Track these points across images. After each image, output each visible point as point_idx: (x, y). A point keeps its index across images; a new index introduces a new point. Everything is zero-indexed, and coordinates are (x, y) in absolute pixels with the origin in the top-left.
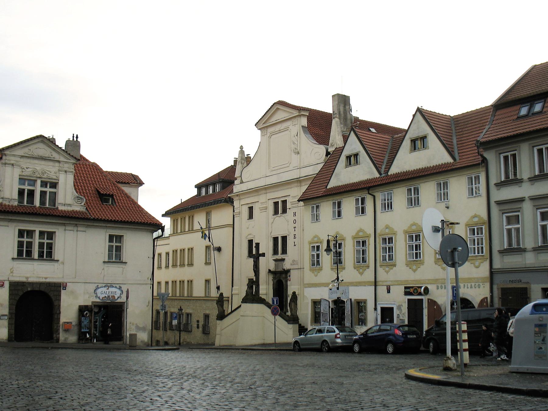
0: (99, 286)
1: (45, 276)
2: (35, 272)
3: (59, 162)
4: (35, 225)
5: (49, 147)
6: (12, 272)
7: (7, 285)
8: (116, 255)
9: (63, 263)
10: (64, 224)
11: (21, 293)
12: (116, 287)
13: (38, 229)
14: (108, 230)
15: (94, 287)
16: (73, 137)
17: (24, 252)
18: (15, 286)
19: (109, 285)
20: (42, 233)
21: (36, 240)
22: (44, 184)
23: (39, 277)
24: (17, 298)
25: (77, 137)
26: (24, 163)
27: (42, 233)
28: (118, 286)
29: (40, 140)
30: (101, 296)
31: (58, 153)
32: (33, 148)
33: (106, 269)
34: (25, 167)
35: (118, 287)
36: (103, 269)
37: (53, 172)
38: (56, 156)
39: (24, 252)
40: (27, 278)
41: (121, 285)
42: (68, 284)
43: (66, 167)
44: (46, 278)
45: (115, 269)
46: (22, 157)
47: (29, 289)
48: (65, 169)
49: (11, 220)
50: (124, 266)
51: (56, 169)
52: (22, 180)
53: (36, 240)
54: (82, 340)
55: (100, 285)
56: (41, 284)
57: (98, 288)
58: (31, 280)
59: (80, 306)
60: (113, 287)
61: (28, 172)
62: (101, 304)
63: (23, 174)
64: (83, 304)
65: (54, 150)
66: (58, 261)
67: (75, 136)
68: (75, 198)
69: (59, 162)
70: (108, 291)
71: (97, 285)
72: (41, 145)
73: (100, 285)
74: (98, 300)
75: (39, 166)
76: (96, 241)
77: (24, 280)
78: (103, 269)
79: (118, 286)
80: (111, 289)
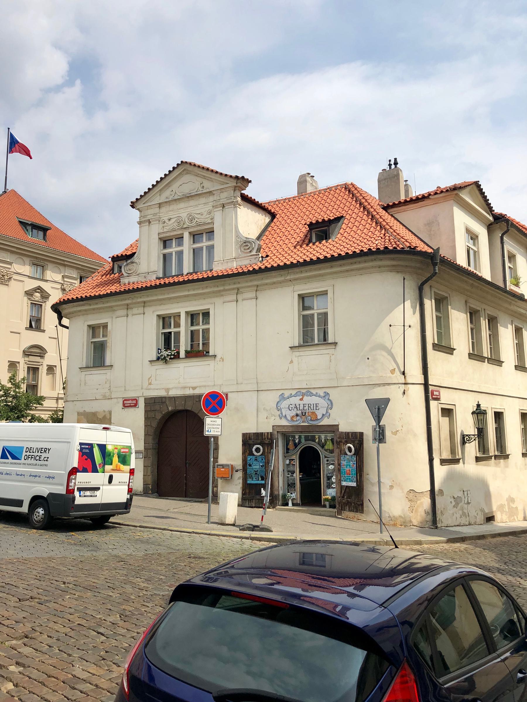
0: (286, 396)
1: (194, 385)
2: (184, 379)
3: (210, 193)
4: (175, 305)
5: (197, 175)
6: (150, 384)
7: (142, 403)
8: (314, 332)
9: (222, 359)
10: (218, 294)
11: (159, 416)
12: (316, 395)
13: (182, 309)
14: (297, 287)
15: (274, 397)
16: (390, 165)
17: (168, 350)
18: (152, 404)
19: (304, 391)
20: (193, 317)
21: (184, 330)
22: (195, 236)
24: (154, 424)
25: (396, 163)
26: (166, 213)
27: (193, 317)
28: (321, 392)
30: (290, 414)
31: (210, 179)
32: (175, 186)
33: (295, 360)
34: (166, 219)
35: (322, 394)
36: (292, 362)
37: (206, 213)
38: (209, 186)
39: (168, 350)
40: (167, 390)
41: (327, 390)
42: (230, 395)
44: (194, 388)
45: (315, 358)
46: (160, 205)
47: (170, 409)
48: (222, 202)
50: (331, 351)
51: (209, 207)
52: (165, 242)
53: (184, 330)
54: (250, 500)
55: (287, 394)
56: (186, 398)
57: (282, 398)
58: (173, 393)
59: (244, 435)
60: (311, 395)
62: (291, 430)
63: (165, 230)
64: (252, 429)
65: (204, 177)
67: (392, 162)
68: (241, 246)
69: (210, 193)
70: (302, 403)
71: (280, 392)
72: (186, 178)
73: (287, 394)
74: (284, 423)
75: (183, 212)
77: (162, 393)
78: (292, 362)
79: (321, 392)
80: (307, 400)
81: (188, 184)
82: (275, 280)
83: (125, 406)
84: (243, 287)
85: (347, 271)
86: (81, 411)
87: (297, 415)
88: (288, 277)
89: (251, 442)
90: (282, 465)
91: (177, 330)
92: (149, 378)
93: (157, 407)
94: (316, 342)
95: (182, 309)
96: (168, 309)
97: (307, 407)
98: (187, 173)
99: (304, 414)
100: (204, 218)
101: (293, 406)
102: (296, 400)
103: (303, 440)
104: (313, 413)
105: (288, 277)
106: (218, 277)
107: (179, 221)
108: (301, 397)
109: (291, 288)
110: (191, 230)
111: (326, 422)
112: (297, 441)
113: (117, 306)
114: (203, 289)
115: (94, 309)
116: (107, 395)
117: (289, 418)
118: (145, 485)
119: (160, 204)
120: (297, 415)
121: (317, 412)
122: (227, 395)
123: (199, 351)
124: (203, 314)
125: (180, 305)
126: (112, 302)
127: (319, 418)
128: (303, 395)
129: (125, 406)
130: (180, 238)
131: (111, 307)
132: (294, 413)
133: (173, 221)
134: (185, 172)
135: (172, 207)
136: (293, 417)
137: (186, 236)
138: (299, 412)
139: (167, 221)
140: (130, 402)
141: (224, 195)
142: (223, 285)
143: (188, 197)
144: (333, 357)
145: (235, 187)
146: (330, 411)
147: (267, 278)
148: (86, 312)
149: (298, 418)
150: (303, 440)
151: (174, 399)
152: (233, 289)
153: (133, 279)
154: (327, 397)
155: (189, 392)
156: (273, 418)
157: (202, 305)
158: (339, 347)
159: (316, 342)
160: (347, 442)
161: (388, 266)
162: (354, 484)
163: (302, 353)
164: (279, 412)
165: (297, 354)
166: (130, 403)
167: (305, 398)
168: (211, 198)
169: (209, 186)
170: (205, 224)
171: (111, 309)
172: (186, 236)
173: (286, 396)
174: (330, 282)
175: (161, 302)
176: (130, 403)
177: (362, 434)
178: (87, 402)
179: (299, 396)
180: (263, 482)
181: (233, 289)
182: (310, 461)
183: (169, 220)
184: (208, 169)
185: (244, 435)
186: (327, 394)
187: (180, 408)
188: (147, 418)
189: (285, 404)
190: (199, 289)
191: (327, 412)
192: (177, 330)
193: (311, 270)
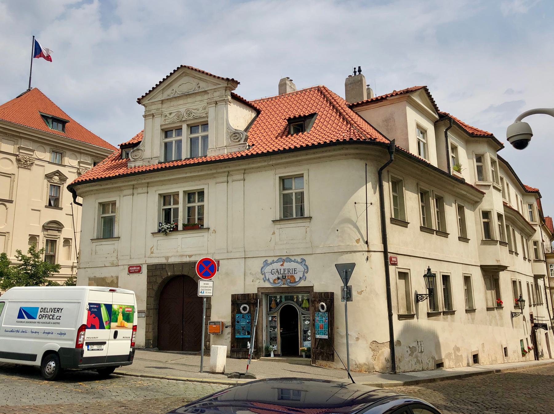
0: (269, 262)
2: (182, 248)
5: (194, 77)
6: (152, 253)
7: (145, 270)
8: (292, 209)
9: (215, 231)
10: (212, 176)
11: (159, 281)
12: (295, 261)
13: (180, 189)
14: (278, 171)
16: (355, 72)
17: (168, 224)
18: (154, 270)
19: (284, 258)
20: (190, 195)
21: (181, 206)
22: (192, 128)
23: (182, 256)
24: (156, 288)
25: (360, 71)
26: (167, 109)
28: (299, 259)
29: (180, 72)
30: (272, 277)
32: (175, 86)
33: (277, 232)
34: (167, 113)
35: (299, 261)
36: (274, 233)
38: (204, 86)
39: (168, 224)
40: (167, 258)
42: (221, 262)
43: (216, 95)
44: (190, 256)
45: (293, 230)
46: (162, 102)
47: (169, 274)
49: (148, 185)
50: (307, 224)
51: (204, 104)
52: (167, 133)
53: (181, 206)
54: (238, 352)
55: (270, 260)
57: (266, 264)
58: (172, 260)
59: (233, 296)
60: (291, 261)
61: (170, 121)
63: (167, 123)
64: (240, 291)
65: (200, 79)
66: (208, 229)
67: (357, 70)
68: (231, 137)
70: (282, 268)
71: (265, 259)
72: (185, 79)
73: (270, 260)
75: (181, 107)
76: (261, 191)
77: (163, 261)
78: (274, 233)
79: (299, 259)
80: (287, 265)
81: (186, 84)
82: (259, 165)
83: (130, 272)
84: (233, 171)
85: (320, 158)
86: (92, 276)
87: (278, 278)
88: (271, 163)
89: (239, 302)
90: (265, 321)
91: (175, 206)
92: (151, 249)
93: (158, 273)
94: (294, 216)
95: (180, 189)
96: (168, 189)
97: (286, 272)
98: (186, 76)
99: (284, 278)
100: (200, 113)
101: (275, 271)
102: (277, 266)
103: (283, 300)
104: (292, 276)
105: (271, 163)
106: (211, 162)
107: (179, 115)
108: (282, 263)
109: (273, 172)
110: (189, 123)
111: (302, 284)
112: (278, 301)
113: (124, 186)
114: (198, 171)
115: (104, 189)
116: (115, 262)
117: (272, 282)
118: (147, 340)
119: (162, 101)
120: (278, 278)
121: (295, 276)
122: (218, 262)
123: (195, 224)
124: (199, 193)
125: (178, 185)
126: (120, 183)
127: (297, 280)
128: (284, 261)
129: (130, 272)
130: (179, 130)
131: (120, 187)
132: (275, 277)
133: (173, 115)
134: (184, 74)
135: (172, 103)
136: (275, 280)
137: (184, 127)
138: (280, 276)
139: (168, 115)
140: (135, 268)
141: (217, 94)
142: (216, 169)
143: (186, 95)
144: (308, 229)
145: (226, 87)
146: (306, 275)
147: (253, 163)
148: (98, 191)
149: (279, 281)
150: (283, 300)
151: (173, 265)
152: (224, 172)
153: (138, 163)
154: (303, 263)
155: (186, 260)
156: (258, 281)
157: (197, 185)
158: (312, 221)
159: (294, 216)
160: (320, 301)
161: (353, 154)
162: (326, 337)
163: (282, 226)
164: (263, 276)
165: (279, 226)
166: (134, 270)
167: (285, 264)
168: (206, 97)
169: (204, 86)
170: (201, 118)
171: (120, 189)
172: (184, 127)
173: (269, 262)
174: (307, 167)
175: (163, 183)
176: (134, 270)
177: (332, 294)
178: (97, 269)
179: (280, 262)
180: (249, 336)
181: (224, 172)
182: (289, 318)
183: (170, 114)
184: (203, 72)
185: (233, 296)
186: (303, 260)
187: (178, 273)
188: (149, 283)
189: (268, 269)
190: (195, 172)
191: (304, 276)
192: (175, 206)
193: (289, 157)
